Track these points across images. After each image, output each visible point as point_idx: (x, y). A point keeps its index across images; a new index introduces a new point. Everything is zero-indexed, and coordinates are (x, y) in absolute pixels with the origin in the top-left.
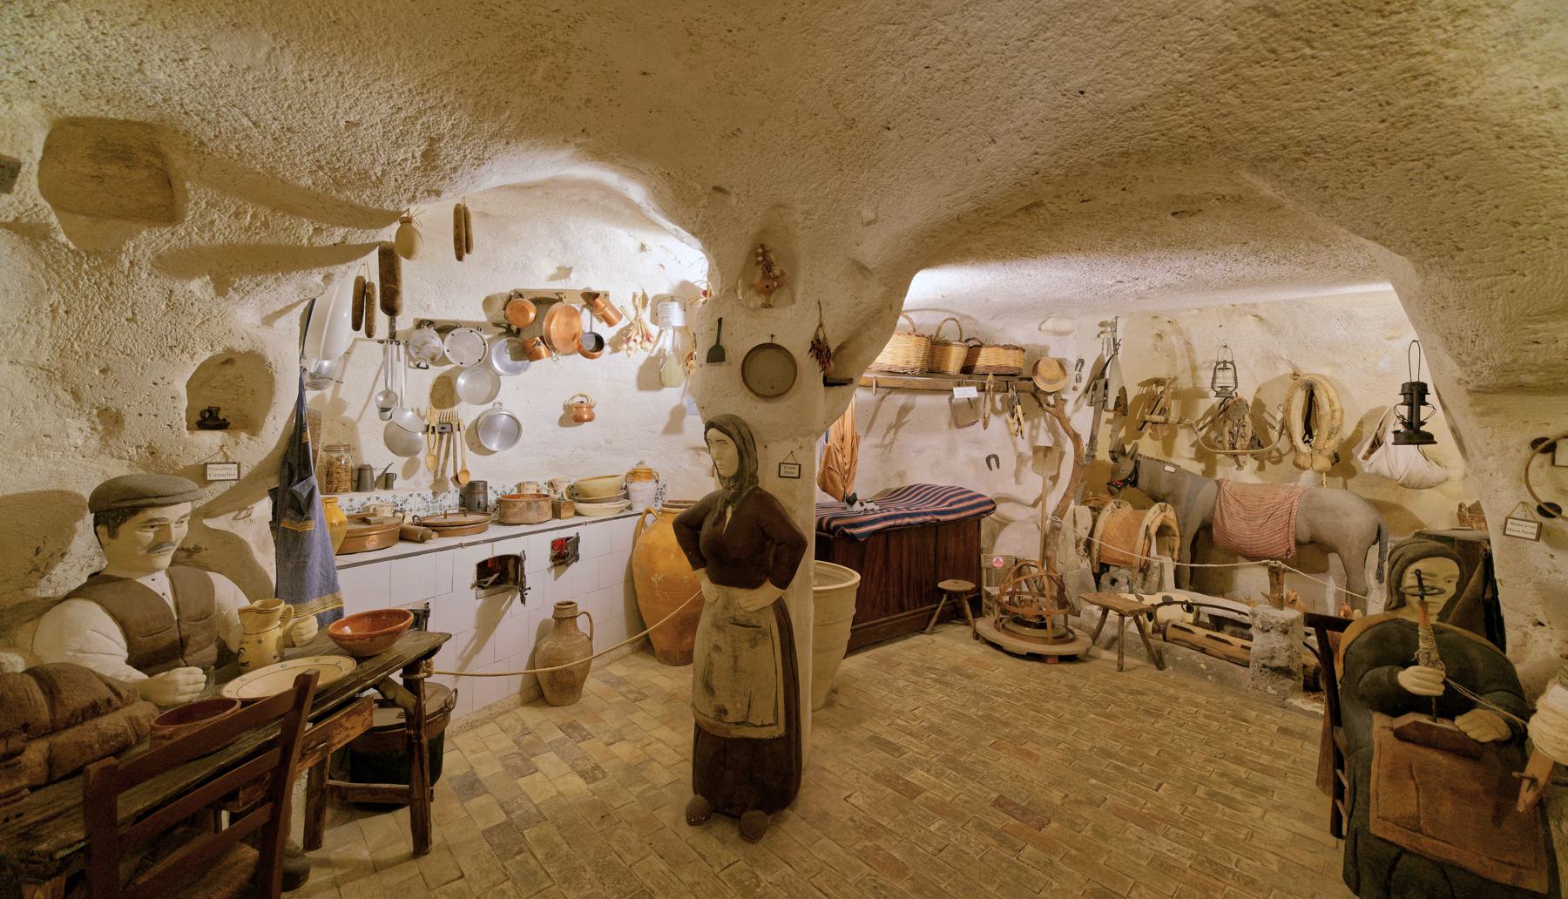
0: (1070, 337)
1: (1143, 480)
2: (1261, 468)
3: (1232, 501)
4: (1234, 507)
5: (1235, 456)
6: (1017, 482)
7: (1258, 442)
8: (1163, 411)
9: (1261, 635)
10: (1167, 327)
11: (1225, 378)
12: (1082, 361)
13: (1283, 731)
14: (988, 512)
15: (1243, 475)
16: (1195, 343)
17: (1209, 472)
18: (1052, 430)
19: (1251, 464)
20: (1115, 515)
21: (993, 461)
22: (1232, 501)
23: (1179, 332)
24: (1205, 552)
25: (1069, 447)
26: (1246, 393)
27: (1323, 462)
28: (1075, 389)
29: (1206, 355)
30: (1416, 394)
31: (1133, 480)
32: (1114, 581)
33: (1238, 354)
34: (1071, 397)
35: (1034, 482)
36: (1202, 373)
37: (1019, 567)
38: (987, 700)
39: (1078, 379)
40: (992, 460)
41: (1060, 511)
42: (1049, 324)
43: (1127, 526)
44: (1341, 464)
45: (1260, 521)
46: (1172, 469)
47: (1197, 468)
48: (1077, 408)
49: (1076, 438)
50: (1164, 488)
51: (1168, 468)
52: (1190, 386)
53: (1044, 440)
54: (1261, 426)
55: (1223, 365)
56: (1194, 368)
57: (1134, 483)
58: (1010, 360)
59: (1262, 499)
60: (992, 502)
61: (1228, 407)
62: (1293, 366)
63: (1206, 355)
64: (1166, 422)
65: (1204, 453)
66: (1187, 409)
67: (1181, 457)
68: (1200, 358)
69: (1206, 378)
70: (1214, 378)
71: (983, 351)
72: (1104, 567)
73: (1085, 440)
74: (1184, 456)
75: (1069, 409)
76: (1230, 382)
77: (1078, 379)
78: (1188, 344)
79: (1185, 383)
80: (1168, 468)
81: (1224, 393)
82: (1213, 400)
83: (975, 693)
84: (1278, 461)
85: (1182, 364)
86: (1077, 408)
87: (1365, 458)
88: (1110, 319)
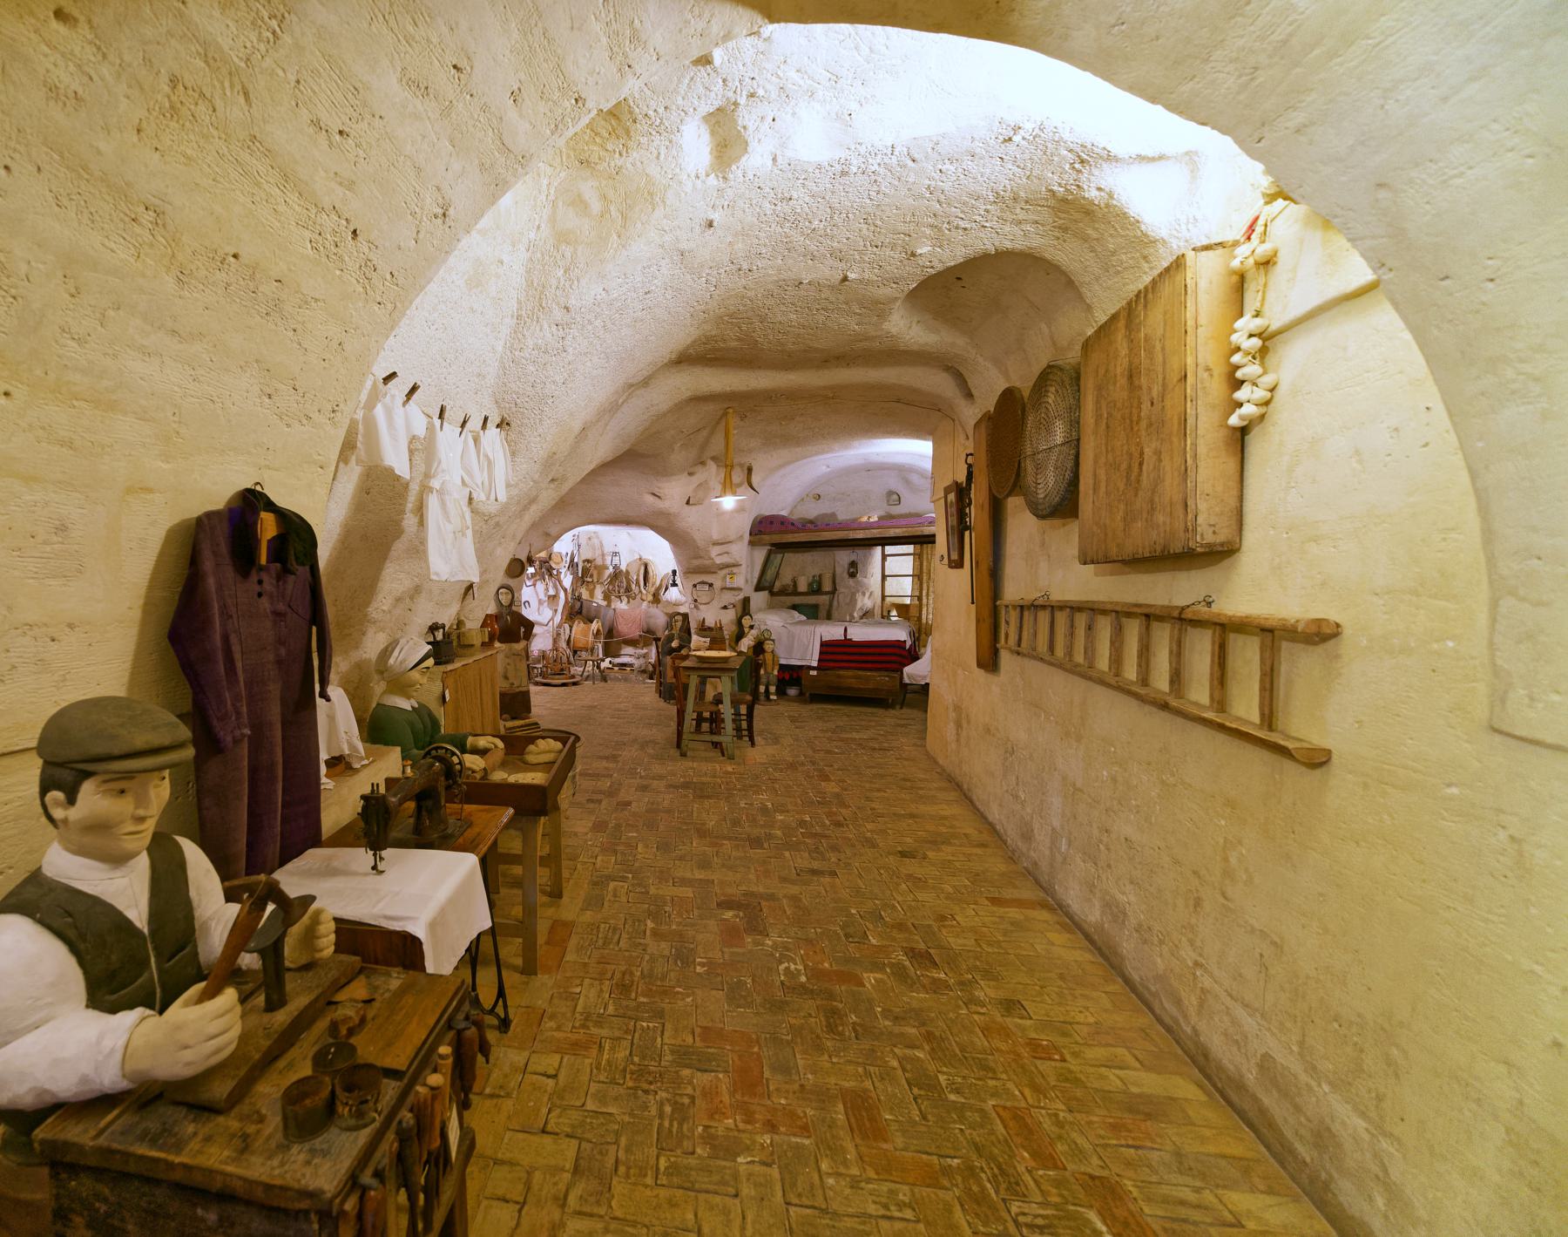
7: (628, 590)
15: (621, 605)
17: (609, 605)
18: (555, 587)
19: (625, 599)
20: (579, 627)
24: (612, 640)
25: (562, 595)
26: (623, 568)
27: (650, 598)
29: (608, 549)
30: (674, 572)
31: (580, 612)
34: (563, 571)
35: (548, 613)
37: (543, 656)
43: (582, 632)
44: (656, 599)
47: (604, 603)
50: (593, 613)
53: (552, 592)
54: (629, 581)
55: (615, 554)
61: (617, 574)
63: (608, 549)
65: (607, 597)
66: (600, 575)
74: (599, 598)
79: (599, 562)
81: (615, 567)
85: (598, 552)
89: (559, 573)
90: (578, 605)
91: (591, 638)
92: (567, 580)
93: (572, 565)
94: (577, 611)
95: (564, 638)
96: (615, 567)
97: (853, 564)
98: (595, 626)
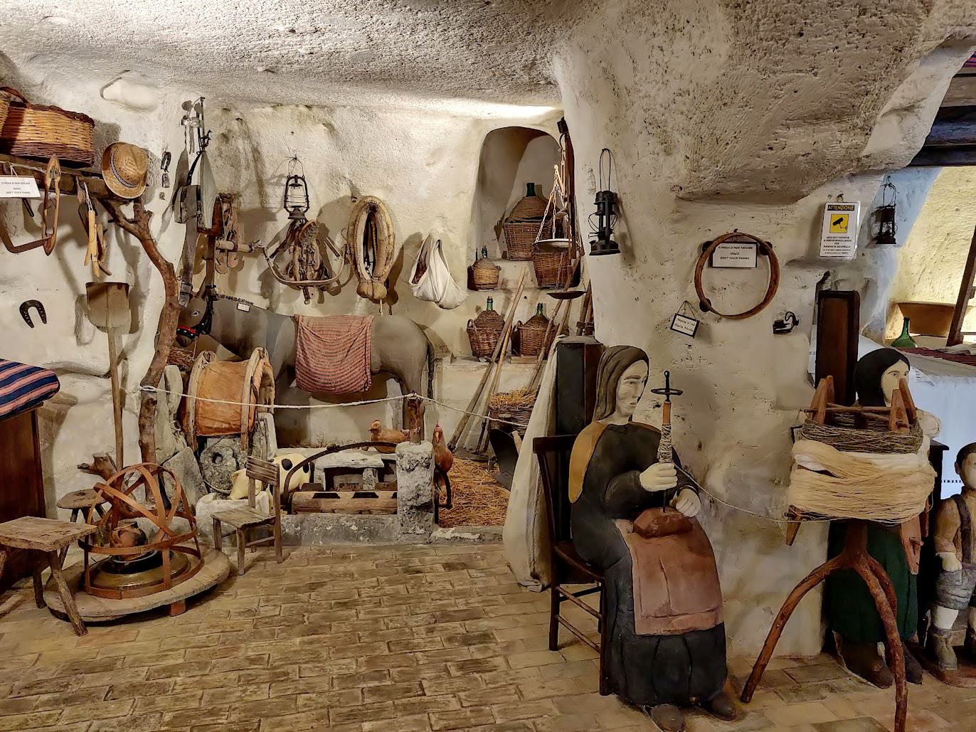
0: (153, 116)
1: (216, 325)
2: (321, 300)
3: (312, 337)
4: (315, 344)
5: (305, 287)
6: (80, 342)
7: (324, 271)
8: (232, 236)
9: (407, 476)
10: (235, 126)
11: (297, 196)
12: (167, 156)
13: (449, 566)
14: (47, 396)
15: (307, 310)
16: (265, 150)
20: (210, 370)
21: (33, 312)
22: (312, 337)
23: (247, 135)
28: (162, 196)
29: (276, 166)
31: (205, 325)
32: (216, 456)
33: (310, 169)
36: (269, 190)
38: (162, 690)
39: (165, 179)
40: (30, 310)
41: (153, 377)
42: (117, 89)
45: (340, 357)
46: (246, 308)
47: (261, 303)
48: (163, 229)
49: (166, 269)
51: (241, 307)
52: (258, 205)
55: (295, 181)
56: (261, 184)
57: (208, 329)
58: (75, 139)
59: (339, 333)
60: (53, 379)
62: (353, 188)
64: (235, 250)
65: (267, 290)
67: (248, 292)
68: (269, 171)
69: (275, 196)
70: (286, 196)
71: (28, 116)
72: (200, 443)
73: (177, 267)
75: (155, 225)
76: (301, 201)
77: (165, 179)
78: (256, 151)
80: (241, 307)
82: (283, 221)
83: (133, 689)
84: (336, 292)
86: (163, 229)
87: (414, 282)
88: (194, 99)
89: (142, 217)
90: (200, 308)
91: (247, 403)
92: (171, 240)
93: (185, 194)
94: (197, 327)
95: (167, 407)
96: (296, 214)
97: (886, 214)
98: (256, 366)
